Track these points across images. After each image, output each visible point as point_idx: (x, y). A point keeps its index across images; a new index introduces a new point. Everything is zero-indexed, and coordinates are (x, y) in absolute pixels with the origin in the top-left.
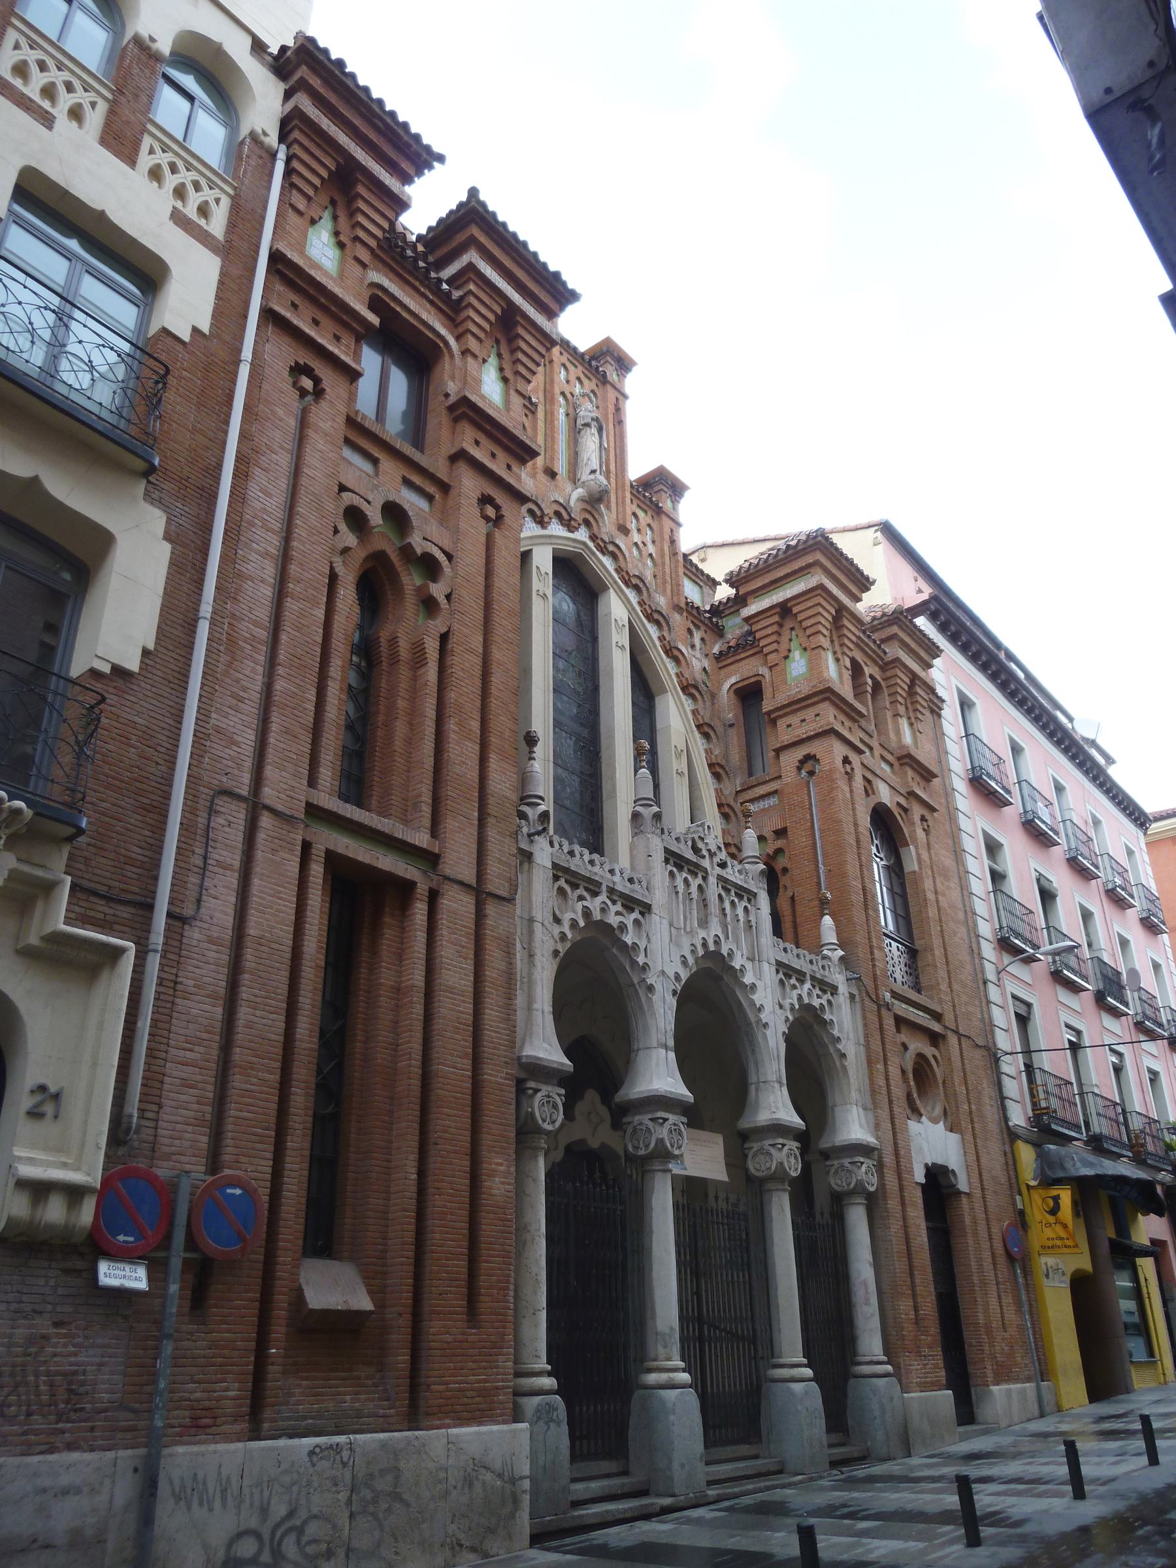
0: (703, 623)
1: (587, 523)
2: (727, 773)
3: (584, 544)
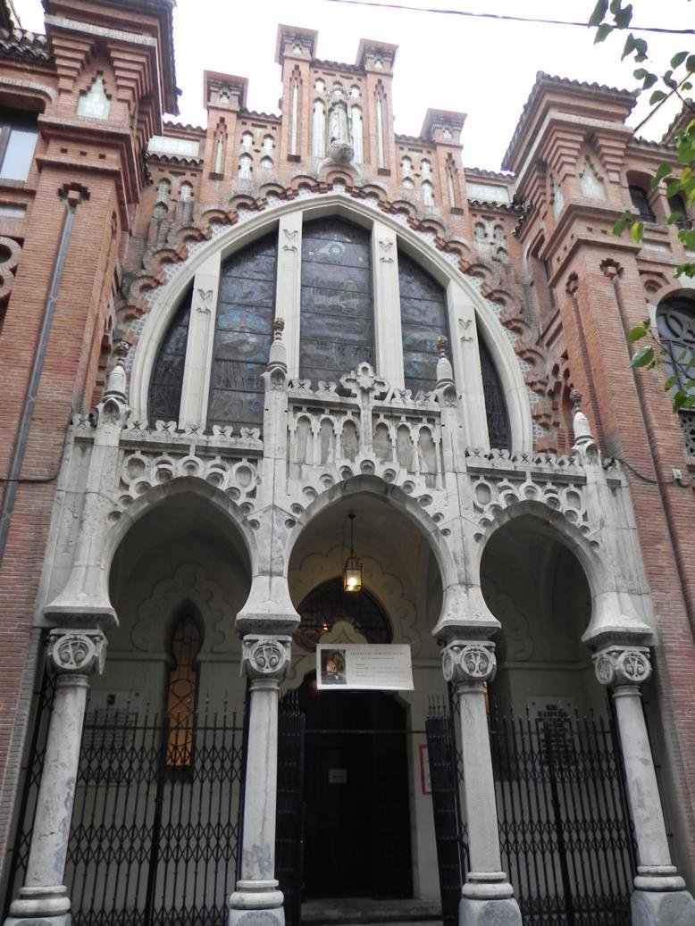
1: (341, 181)
2: (526, 324)
3: (339, 197)
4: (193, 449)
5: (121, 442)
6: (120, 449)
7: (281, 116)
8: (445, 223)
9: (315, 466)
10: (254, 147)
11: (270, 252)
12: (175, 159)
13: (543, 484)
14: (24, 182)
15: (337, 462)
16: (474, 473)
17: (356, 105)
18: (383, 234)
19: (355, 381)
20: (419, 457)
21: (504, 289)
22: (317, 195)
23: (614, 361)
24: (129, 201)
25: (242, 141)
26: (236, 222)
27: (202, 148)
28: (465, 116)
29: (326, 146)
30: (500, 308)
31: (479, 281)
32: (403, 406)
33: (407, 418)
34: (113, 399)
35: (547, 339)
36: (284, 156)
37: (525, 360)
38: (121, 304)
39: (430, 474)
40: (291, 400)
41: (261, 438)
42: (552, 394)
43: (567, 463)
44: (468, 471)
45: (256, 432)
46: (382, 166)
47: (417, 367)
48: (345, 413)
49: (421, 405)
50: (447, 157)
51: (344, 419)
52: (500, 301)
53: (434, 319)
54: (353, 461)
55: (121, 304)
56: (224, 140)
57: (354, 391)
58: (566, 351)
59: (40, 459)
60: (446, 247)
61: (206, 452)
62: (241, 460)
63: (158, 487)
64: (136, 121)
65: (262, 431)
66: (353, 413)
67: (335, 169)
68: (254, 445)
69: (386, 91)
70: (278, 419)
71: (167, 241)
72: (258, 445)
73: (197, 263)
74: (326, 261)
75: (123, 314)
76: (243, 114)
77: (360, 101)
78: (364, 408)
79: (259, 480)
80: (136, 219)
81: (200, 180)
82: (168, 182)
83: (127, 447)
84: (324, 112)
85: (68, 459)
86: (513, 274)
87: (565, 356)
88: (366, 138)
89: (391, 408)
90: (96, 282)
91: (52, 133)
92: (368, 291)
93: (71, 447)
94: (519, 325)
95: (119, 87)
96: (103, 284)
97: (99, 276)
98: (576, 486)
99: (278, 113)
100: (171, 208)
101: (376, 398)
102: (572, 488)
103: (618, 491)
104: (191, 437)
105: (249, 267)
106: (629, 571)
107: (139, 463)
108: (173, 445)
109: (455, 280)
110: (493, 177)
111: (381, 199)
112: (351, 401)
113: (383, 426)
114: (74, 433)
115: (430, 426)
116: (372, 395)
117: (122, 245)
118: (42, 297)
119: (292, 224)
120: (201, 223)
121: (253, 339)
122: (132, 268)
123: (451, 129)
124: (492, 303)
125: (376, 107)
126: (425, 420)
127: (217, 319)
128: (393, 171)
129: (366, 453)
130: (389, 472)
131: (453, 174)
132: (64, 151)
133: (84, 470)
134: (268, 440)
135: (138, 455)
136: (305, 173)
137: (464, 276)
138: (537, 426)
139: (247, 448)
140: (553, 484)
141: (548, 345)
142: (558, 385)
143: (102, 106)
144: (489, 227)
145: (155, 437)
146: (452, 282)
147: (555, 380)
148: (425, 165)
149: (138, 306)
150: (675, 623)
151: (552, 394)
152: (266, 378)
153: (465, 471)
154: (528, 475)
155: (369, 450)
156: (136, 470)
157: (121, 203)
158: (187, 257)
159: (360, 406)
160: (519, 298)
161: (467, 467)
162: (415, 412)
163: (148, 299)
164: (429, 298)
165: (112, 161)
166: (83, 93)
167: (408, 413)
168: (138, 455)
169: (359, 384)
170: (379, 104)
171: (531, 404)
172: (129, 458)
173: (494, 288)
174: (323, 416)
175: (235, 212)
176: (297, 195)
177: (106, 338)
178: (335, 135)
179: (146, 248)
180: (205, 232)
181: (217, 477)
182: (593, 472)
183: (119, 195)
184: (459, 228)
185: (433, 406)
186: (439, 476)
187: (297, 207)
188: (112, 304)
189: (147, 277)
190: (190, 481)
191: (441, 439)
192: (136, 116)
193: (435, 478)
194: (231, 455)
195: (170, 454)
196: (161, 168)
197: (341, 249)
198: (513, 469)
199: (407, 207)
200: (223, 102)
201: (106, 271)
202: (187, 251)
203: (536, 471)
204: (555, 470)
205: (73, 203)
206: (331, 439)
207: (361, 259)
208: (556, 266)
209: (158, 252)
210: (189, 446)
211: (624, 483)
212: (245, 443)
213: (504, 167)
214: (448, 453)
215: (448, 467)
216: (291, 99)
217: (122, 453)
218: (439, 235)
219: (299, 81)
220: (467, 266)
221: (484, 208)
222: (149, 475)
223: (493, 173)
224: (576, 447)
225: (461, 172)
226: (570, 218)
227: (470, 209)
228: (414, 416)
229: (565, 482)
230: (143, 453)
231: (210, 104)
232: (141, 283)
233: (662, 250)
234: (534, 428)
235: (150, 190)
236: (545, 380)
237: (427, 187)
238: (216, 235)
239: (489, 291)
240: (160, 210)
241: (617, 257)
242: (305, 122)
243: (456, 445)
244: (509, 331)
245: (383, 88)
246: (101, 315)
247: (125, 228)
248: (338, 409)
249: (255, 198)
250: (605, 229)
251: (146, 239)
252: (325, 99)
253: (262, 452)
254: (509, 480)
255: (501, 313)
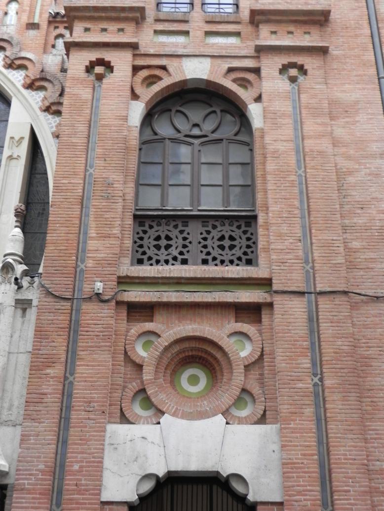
23: (67, 169)
103: (28, 310)
106: (11, 400)
109: (17, 97)
150: (39, 457)
211: (35, 303)
233: (181, 39)
241: (108, 55)
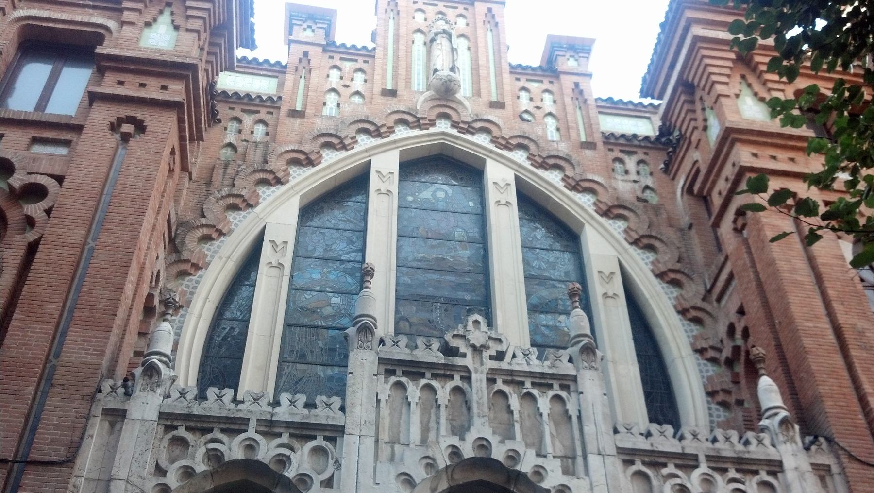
0: (640, 147)
1: (446, 116)
2: (688, 276)
3: (444, 134)
4: (253, 423)
5: (162, 415)
6: (158, 424)
7: (375, 49)
8: (575, 158)
9: (412, 446)
10: (342, 82)
11: (359, 198)
12: (248, 95)
13: (724, 471)
14: (71, 117)
15: (441, 440)
16: (628, 456)
17: (462, 35)
18: (499, 175)
19: (463, 337)
20: (551, 434)
21: (654, 234)
22: (417, 132)
24: (192, 140)
25: (328, 76)
26: (319, 163)
27: (281, 85)
28: (593, 41)
29: (428, 78)
30: (650, 256)
31: (621, 225)
32: (526, 368)
33: (534, 384)
34: (155, 360)
35: (715, 293)
36: (377, 89)
37: (690, 320)
38: (174, 258)
39: (566, 457)
40: (381, 361)
41: (342, 409)
42: (730, 363)
43: (754, 442)
44: (618, 453)
45: (336, 401)
46: (494, 99)
47: (547, 332)
48: (452, 377)
49: (550, 367)
50: (573, 87)
51: (450, 385)
52: (650, 248)
53: (567, 273)
54: (462, 439)
55: (174, 258)
56: (308, 76)
57: (463, 350)
58: (742, 304)
59: (56, 434)
60: (576, 186)
61: (270, 428)
62: (314, 438)
63: (204, 474)
64: (205, 53)
65: (343, 400)
66: (462, 378)
67: (438, 103)
68: (333, 418)
69: (497, 19)
70: (365, 387)
71: (234, 186)
72: (337, 419)
73: (268, 209)
74: (429, 208)
75: (175, 269)
76: (329, 47)
77: (467, 31)
78: (476, 371)
79: (338, 464)
80: (199, 160)
81: (278, 118)
82: (239, 120)
83: (168, 420)
84: (425, 44)
85: (92, 437)
86: (664, 216)
87: (741, 312)
88: (475, 69)
89: (512, 371)
90: (145, 224)
91: (106, 65)
92: (482, 241)
93: (98, 420)
94: (678, 276)
95: (189, 17)
96: (154, 228)
97: (149, 218)
98: (769, 473)
99: (371, 46)
100: (240, 149)
101: (491, 358)
102: (764, 476)
104: (251, 408)
105: (337, 217)
107: (181, 442)
108: (227, 418)
110: (631, 107)
111: (495, 134)
112: (459, 361)
113: (501, 393)
114: (102, 403)
115: (564, 394)
116: (486, 354)
117: (178, 190)
118: (80, 240)
119: (386, 165)
120: (276, 165)
121: (336, 300)
122: (189, 216)
123: (576, 57)
124: (640, 251)
125: (486, 36)
126: (556, 386)
127: (292, 276)
128: (508, 102)
129: (481, 428)
130: (511, 454)
131: (582, 105)
132: (121, 83)
133: (110, 450)
134: (351, 412)
135: (182, 432)
136: (402, 108)
137: (603, 220)
138: (714, 406)
139: (324, 422)
140: (737, 470)
141: (719, 300)
142: (736, 349)
143: (168, 38)
144: (631, 163)
145: (205, 409)
146: (587, 227)
147: (732, 344)
148: (547, 97)
149: (194, 261)
151: (730, 363)
152: (350, 334)
153: (614, 452)
154: (702, 458)
155: (483, 424)
156: (177, 451)
157: (182, 138)
158: (258, 204)
159: (472, 369)
160: (674, 244)
161: (618, 448)
162: (543, 375)
163: (207, 252)
164: (559, 248)
165: (176, 91)
166: (148, 24)
167: (535, 377)
168: (182, 432)
169: (468, 340)
170: (489, 34)
171: (703, 377)
172: (169, 436)
173: (641, 233)
174: (423, 382)
175: (318, 153)
176: (393, 132)
177: (150, 297)
178: (439, 68)
179: (208, 194)
180: (280, 175)
181: (283, 461)
182: (792, 455)
183: (181, 130)
184: (592, 166)
185: (568, 369)
186: (580, 460)
187: (394, 146)
188: (162, 256)
189: (207, 226)
190: (250, 465)
191: (579, 411)
192: (206, 48)
193: (574, 463)
194: (303, 431)
195: (223, 431)
196: (232, 106)
197: (446, 193)
198: (680, 451)
199: (526, 142)
200: (307, 35)
201: (158, 213)
202: (258, 196)
203: (712, 453)
204: (740, 452)
205: (126, 138)
206: (433, 411)
207: (471, 204)
208: (717, 201)
209: (223, 197)
210: (248, 419)
212: (321, 415)
213: (644, 93)
214: (589, 429)
215: (591, 447)
216: (386, 31)
217: (161, 429)
218: (567, 173)
219: (395, 12)
220: (604, 208)
221: (622, 141)
222: (193, 458)
223: (630, 102)
224: (764, 422)
225: (591, 103)
226: (728, 144)
227: (604, 143)
228: (543, 381)
229: (754, 468)
230: (188, 429)
231: (292, 38)
232: (199, 233)
234: (710, 409)
235: (216, 130)
236: (719, 345)
237: (550, 121)
238: (294, 178)
239: (636, 236)
240: (228, 152)
242: (402, 54)
243: (599, 418)
244: (665, 285)
245: (493, 16)
246: (147, 265)
247: (184, 168)
248: (442, 372)
249: (342, 136)
250: (774, 154)
251: (209, 183)
252: (425, 29)
253: (343, 426)
254: (677, 466)
255: (653, 263)
